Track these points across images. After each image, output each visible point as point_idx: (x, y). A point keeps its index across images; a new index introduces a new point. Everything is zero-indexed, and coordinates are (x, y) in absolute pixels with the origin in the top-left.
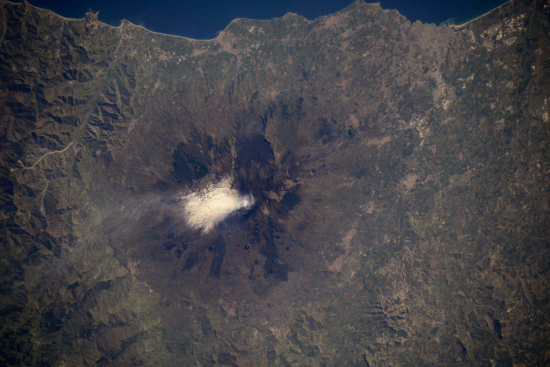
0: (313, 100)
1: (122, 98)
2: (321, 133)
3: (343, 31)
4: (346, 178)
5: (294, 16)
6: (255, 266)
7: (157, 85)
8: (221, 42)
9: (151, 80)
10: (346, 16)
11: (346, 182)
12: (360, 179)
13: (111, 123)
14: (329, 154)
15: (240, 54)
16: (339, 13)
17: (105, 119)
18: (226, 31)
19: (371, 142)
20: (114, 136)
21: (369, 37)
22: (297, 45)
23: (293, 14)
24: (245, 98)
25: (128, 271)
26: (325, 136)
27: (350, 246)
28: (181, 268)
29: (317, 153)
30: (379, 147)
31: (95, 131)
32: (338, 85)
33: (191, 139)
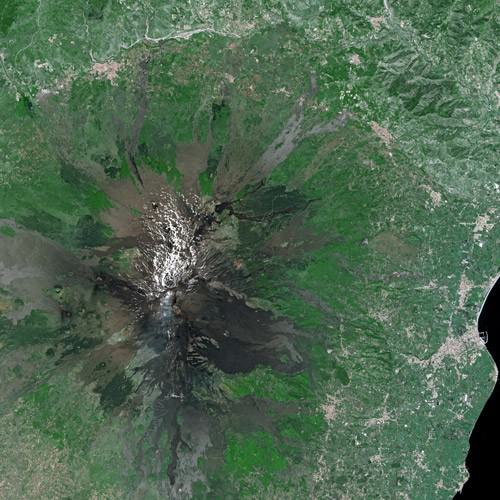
5: (458, 487)
8: (465, 337)
15: (430, 367)
18: (482, 352)
22: (402, 479)
23: (461, 485)
24: (346, 353)
28: (69, 157)
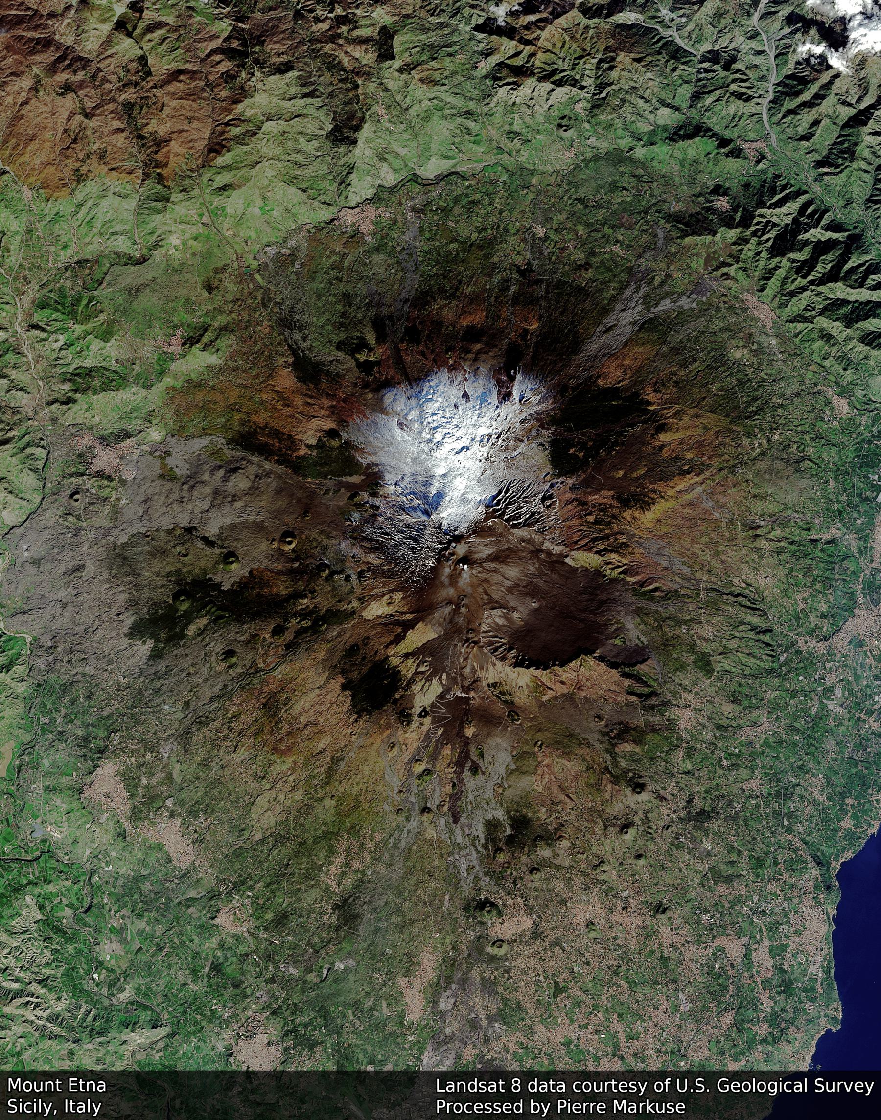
0: (621, 822)
1: (844, 302)
2: (521, 823)
3: (773, 952)
4: (357, 865)
6: (217, 551)
7: (842, 405)
9: (859, 394)
10: (812, 969)
11: (347, 865)
12: (336, 907)
13: (792, 256)
14: (451, 831)
15: (830, 653)
16: (828, 949)
17: (806, 243)
19: (429, 962)
20: (751, 254)
21: (728, 1019)
24: (708, 631)
25: (353, 204)
26: (509, 831)
27: (145, 840)
28: (303, 345)
29: (471, 797)
30: (402, 982)
31: (784, 210)
32: (633, 903)
33: (665, 453)
